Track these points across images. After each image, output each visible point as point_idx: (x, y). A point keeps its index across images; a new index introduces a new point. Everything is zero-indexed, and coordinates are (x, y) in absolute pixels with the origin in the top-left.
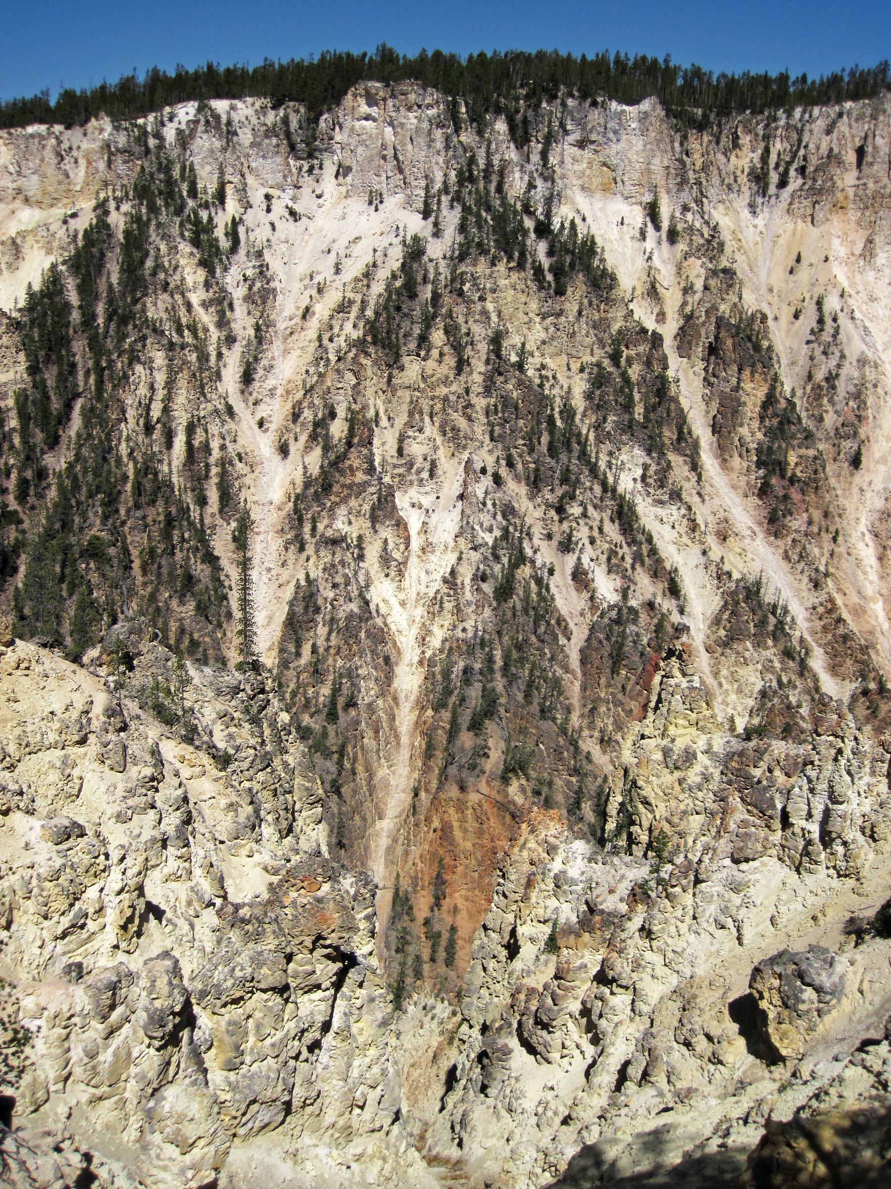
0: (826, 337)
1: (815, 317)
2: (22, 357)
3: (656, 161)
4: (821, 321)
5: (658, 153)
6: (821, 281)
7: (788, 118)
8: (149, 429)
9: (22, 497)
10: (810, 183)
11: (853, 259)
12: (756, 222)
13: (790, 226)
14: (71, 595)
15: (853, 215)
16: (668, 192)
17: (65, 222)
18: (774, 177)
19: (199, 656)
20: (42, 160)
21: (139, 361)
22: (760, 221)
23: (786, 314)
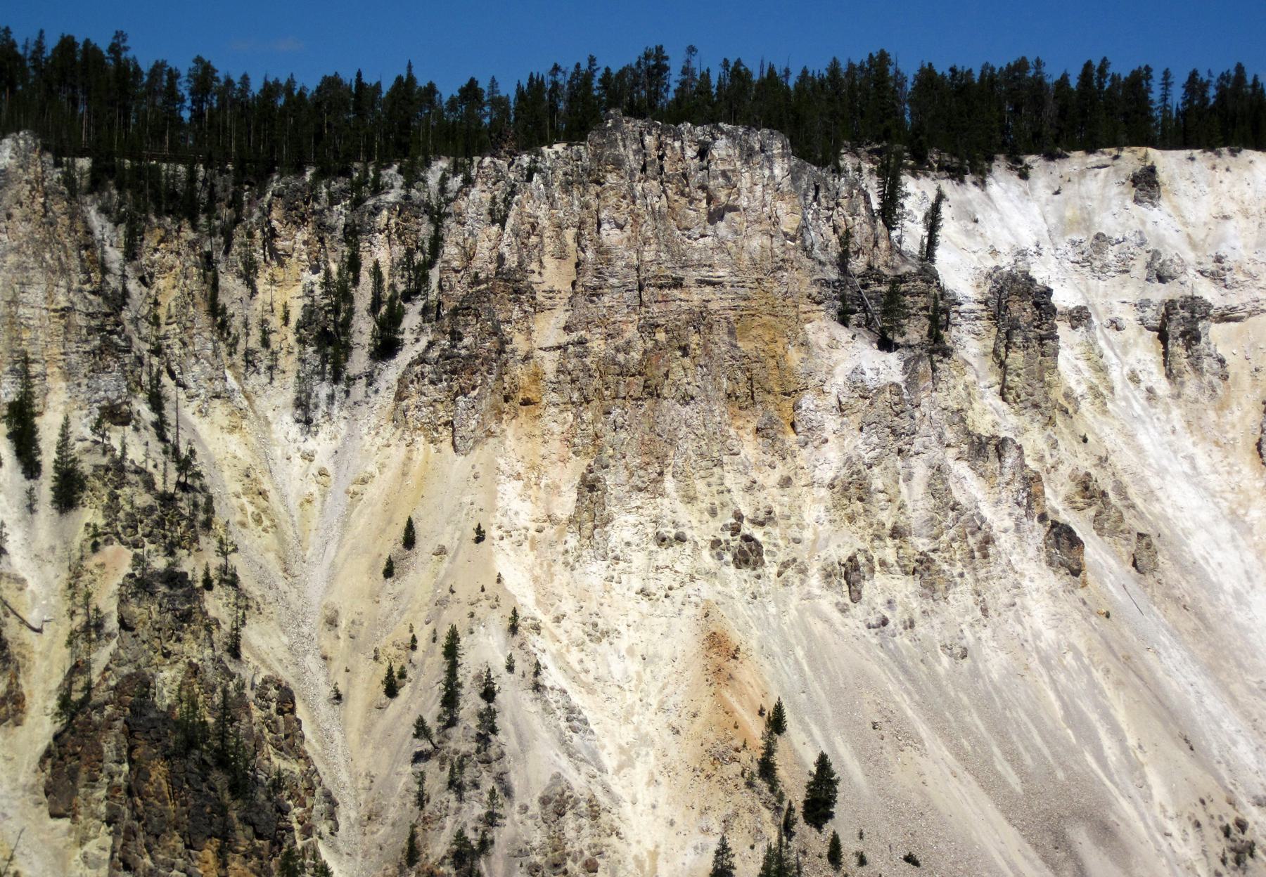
0: (461, 741)
1: (438, 691)
3: (35, 295)
4: (450, 699)
5: (38, 276)
6: (461, 594)
7: (408, 185)
10: (445, 342)
11: (550, 531)
12: (311, 444)
13: (397, 453)
15: (556, 421)
16: (69, 373)
18: (363, 329)
22: (321, 444)
23: (365, 684)
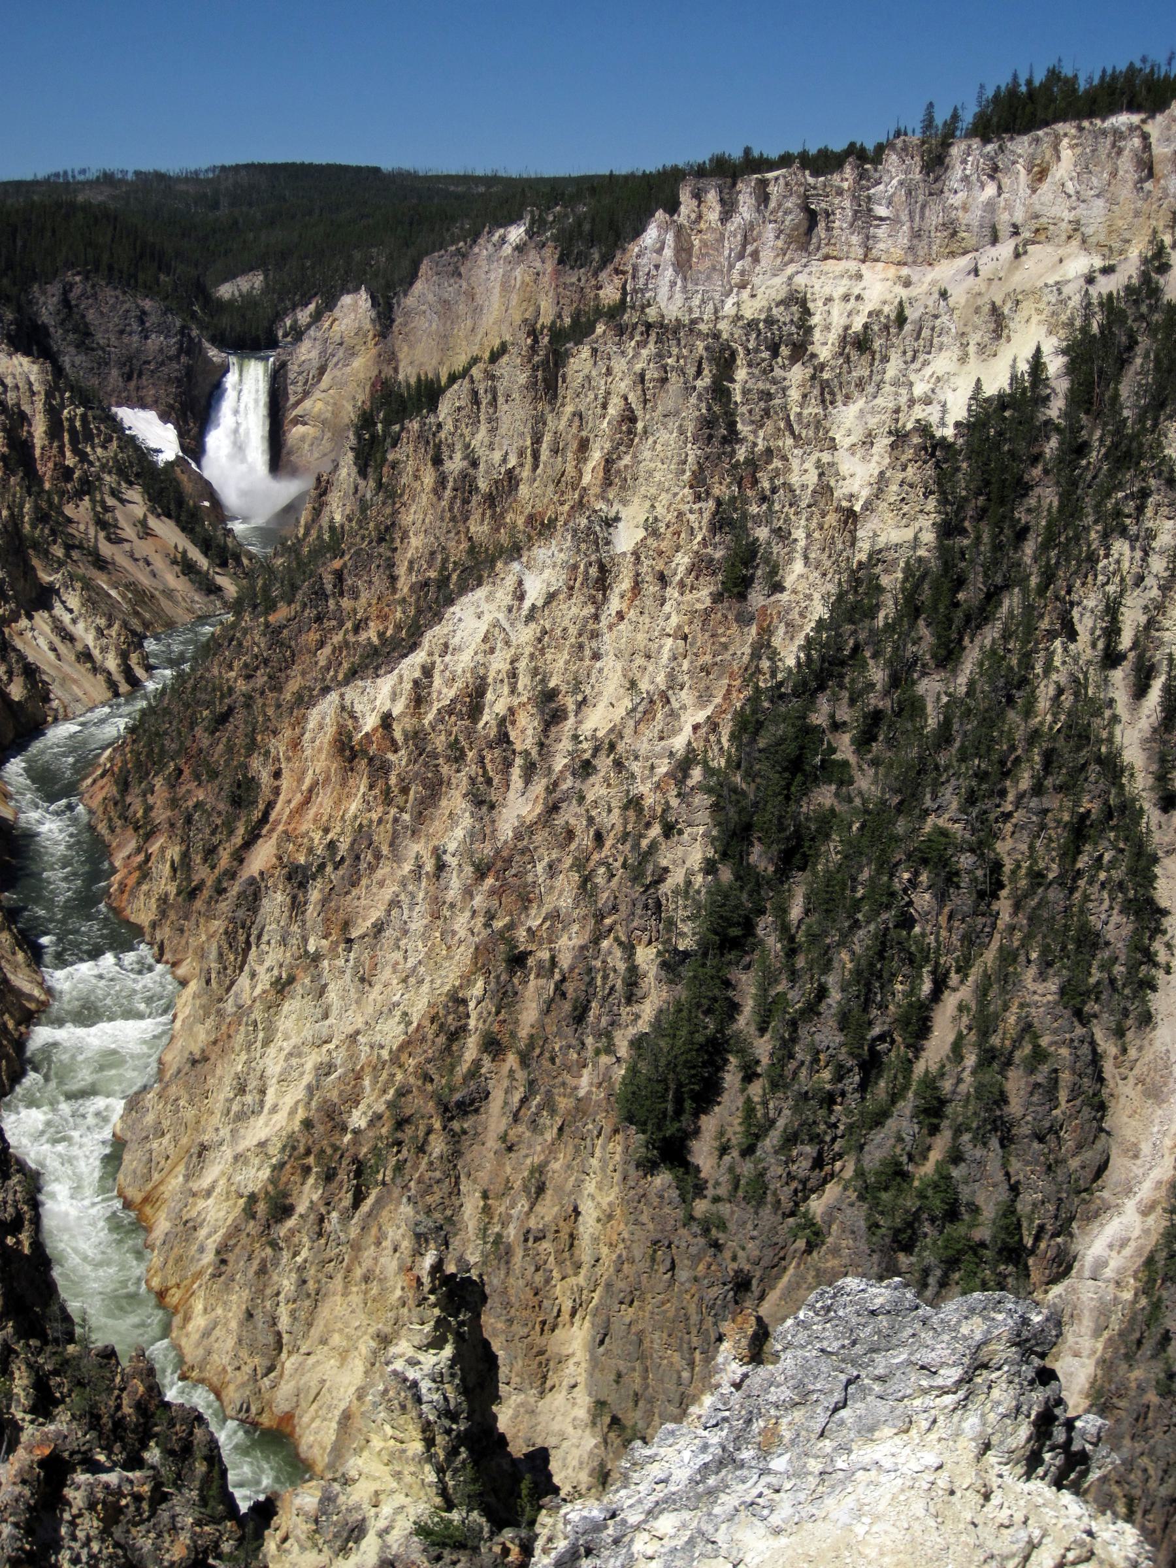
2: (931, 504)
8: (1112, 659)
9: (864, 741)
14: (868, 923)
17: (1090, 280)
19: (1040, 1078)
20: (1114, 174)
21: (1124, 532)
